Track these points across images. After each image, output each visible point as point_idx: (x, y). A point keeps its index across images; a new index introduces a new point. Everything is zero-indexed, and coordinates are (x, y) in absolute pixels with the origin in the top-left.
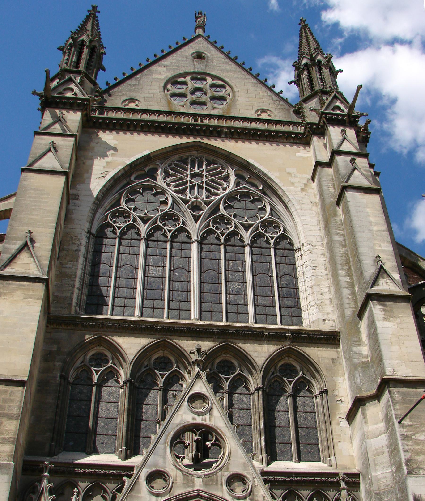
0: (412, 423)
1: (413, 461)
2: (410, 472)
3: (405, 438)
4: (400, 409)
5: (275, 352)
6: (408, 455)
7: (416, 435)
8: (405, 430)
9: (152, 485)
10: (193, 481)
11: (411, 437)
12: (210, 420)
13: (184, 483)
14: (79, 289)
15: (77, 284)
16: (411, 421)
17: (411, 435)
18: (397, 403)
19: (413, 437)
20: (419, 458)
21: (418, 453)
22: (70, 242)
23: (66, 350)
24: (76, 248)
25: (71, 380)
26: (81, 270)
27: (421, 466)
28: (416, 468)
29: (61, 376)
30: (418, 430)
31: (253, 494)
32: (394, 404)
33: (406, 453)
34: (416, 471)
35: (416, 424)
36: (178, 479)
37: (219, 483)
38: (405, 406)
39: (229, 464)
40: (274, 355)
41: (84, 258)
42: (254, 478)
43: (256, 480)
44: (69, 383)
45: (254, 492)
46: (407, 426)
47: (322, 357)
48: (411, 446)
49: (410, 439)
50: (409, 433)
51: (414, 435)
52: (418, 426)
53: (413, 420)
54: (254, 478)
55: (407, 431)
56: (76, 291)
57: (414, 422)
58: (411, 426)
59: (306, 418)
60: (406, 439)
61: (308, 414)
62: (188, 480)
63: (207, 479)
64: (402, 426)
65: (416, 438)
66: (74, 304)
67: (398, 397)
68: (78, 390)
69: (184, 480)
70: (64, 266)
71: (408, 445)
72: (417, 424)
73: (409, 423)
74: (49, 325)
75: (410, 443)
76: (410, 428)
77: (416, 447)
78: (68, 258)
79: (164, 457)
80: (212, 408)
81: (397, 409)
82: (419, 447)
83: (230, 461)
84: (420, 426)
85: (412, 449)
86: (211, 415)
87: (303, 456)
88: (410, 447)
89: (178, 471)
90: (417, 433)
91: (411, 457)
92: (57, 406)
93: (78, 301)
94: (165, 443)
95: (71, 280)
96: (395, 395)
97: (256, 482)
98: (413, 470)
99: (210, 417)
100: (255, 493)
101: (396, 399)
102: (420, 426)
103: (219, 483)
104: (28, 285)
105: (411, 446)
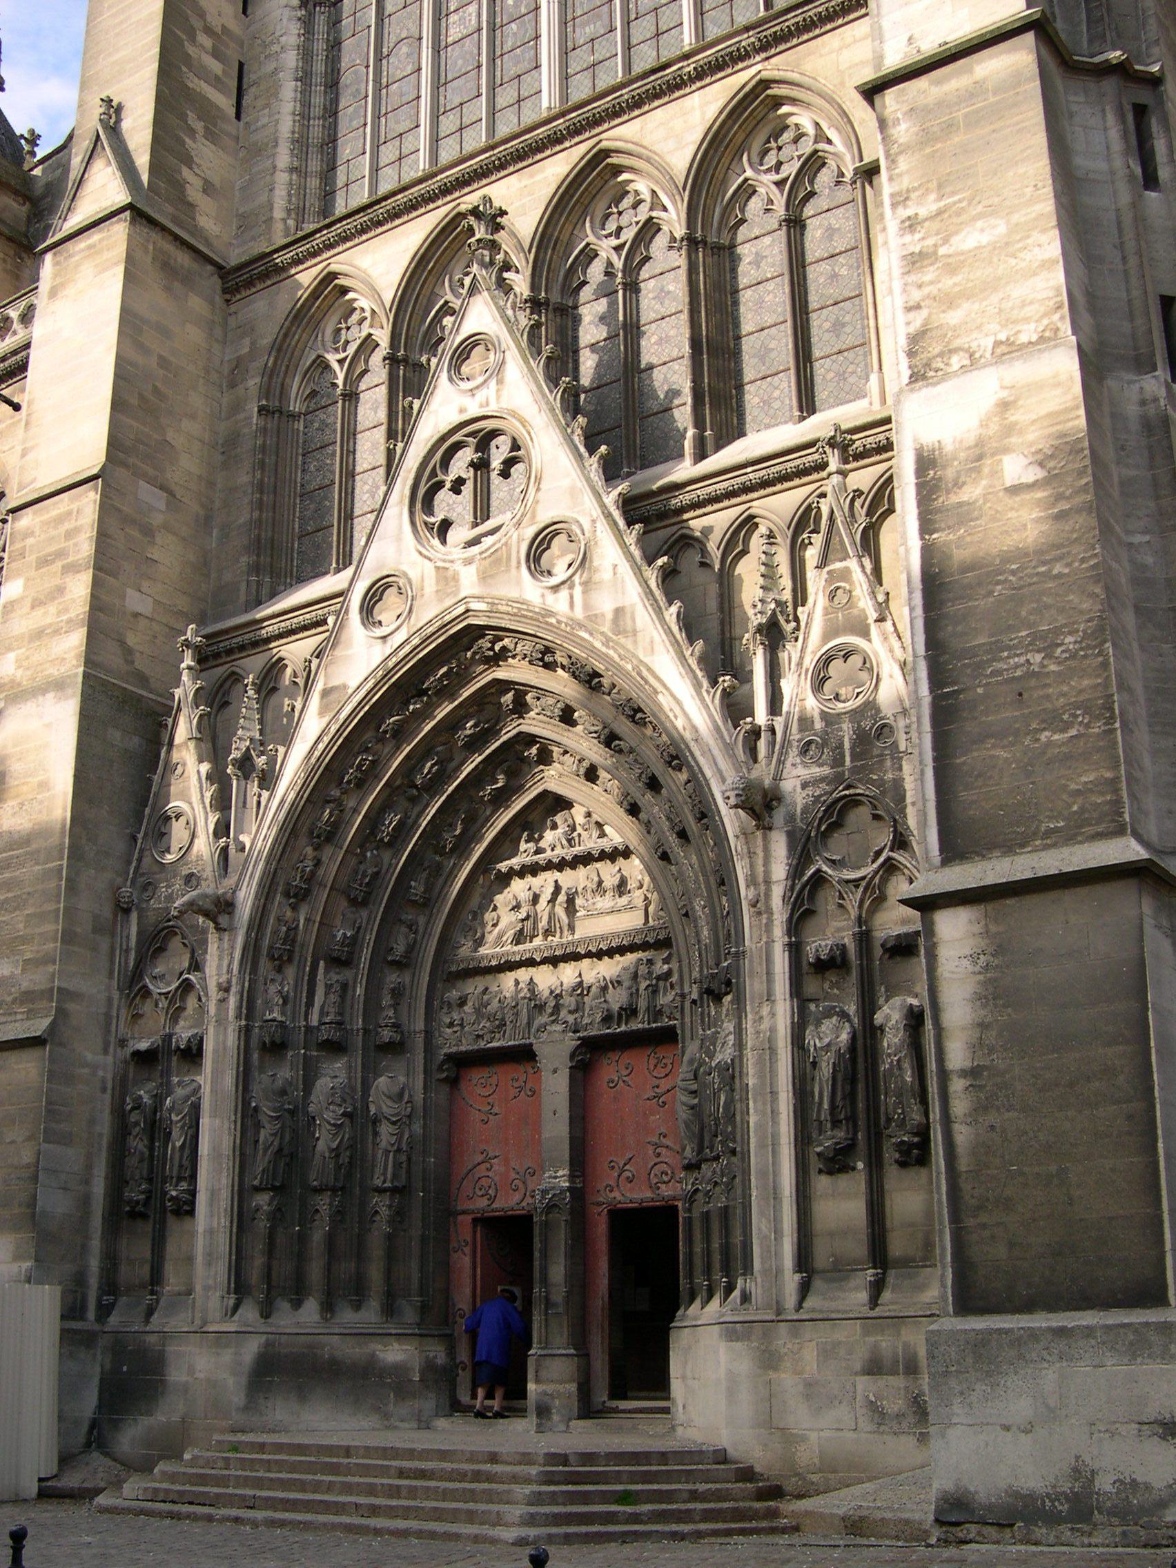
0: (942, 204)
1: (934, 333)
2: (917, 377)
3: (914, 263)
4: (908, 172)
5: (721, 112)
6: (918, 319)
7: (954, 240)
8: (917, 236)
9: (379, 618)
10: (455, 578)
11: (935, 253)
12: (498, 397)
13: (437, 591)
14: (292, 170)
15: (284, 158)
16: (941, 197)
17: (935, 245)
18: (901, 153)
19: (942, 251)
20: (953, 317)
21: (949, 301)
22: (263, 56)
23: (266, 341)
24: (274, 65)
25: (295, 406)
26: (290, 118)
27: (957, 343)
28: (941, 355)
29: (261, 410)
30: (964, 217)
31: (590, 568)
32: (893, 161)
33: (912, 315)
34: (941, 365)
35: (955, 203)
36: (426, 583)
37: (514, 563)
38: (928, 150)
39: (537, 502)
40: (718, 124)
41: (297, 80)
42: (594, 521)
43: (598, 524)
44: (293, 416)
45: (591, 561)
46: (926, 219)
47: (850, 68)
48: (931, 283)
49: (930, 261)
50: (930, 242)
51: (946, 241)
52: (964, 204)
53: (948, 190)
54: (594, 521)
55: (923, 238)
56: (282, 178)
57: (953, 193)
58: (940, 213)
59: (834, 276)
60: (918, 265)
61: (841, 259)
62: (446, 578)
63: (488, 561)
64: (910, 226)
65: (951, 251)
66: (278, 214)
67: (907, 131)
68: (316, 425)
69: (438, 582)
70: (253, 128)
71: (920, 287)
72: (960, 201)
73: (934, 208)
74: (228, 297)
75: (929, 275)
76: (935, 225)
77: (948, 283)
78: (259, 103)
79: (399, 538)
80: (503, 362)
81: (900, 175)
82: (957, 279)
83: (540, 494)
84: (969, 204)
85: (935, 292)
86: (500, 382)
87: (821, 394)
88: (926, 290)
89: (426, 561)
90: (956, 233)
91: (926, 322)
92: (261, 488)
93: (289, 202)
94: (401, 501)
95: (268, 157)
96: (898, 128)
97: (598, 533)
98: (927, 365)
99: (498, 391)
100: (595, 564)
101: (901, 141)
102: (969, 204)
103: (514, 563)
104: (100, 241)
105: (931, 283)
